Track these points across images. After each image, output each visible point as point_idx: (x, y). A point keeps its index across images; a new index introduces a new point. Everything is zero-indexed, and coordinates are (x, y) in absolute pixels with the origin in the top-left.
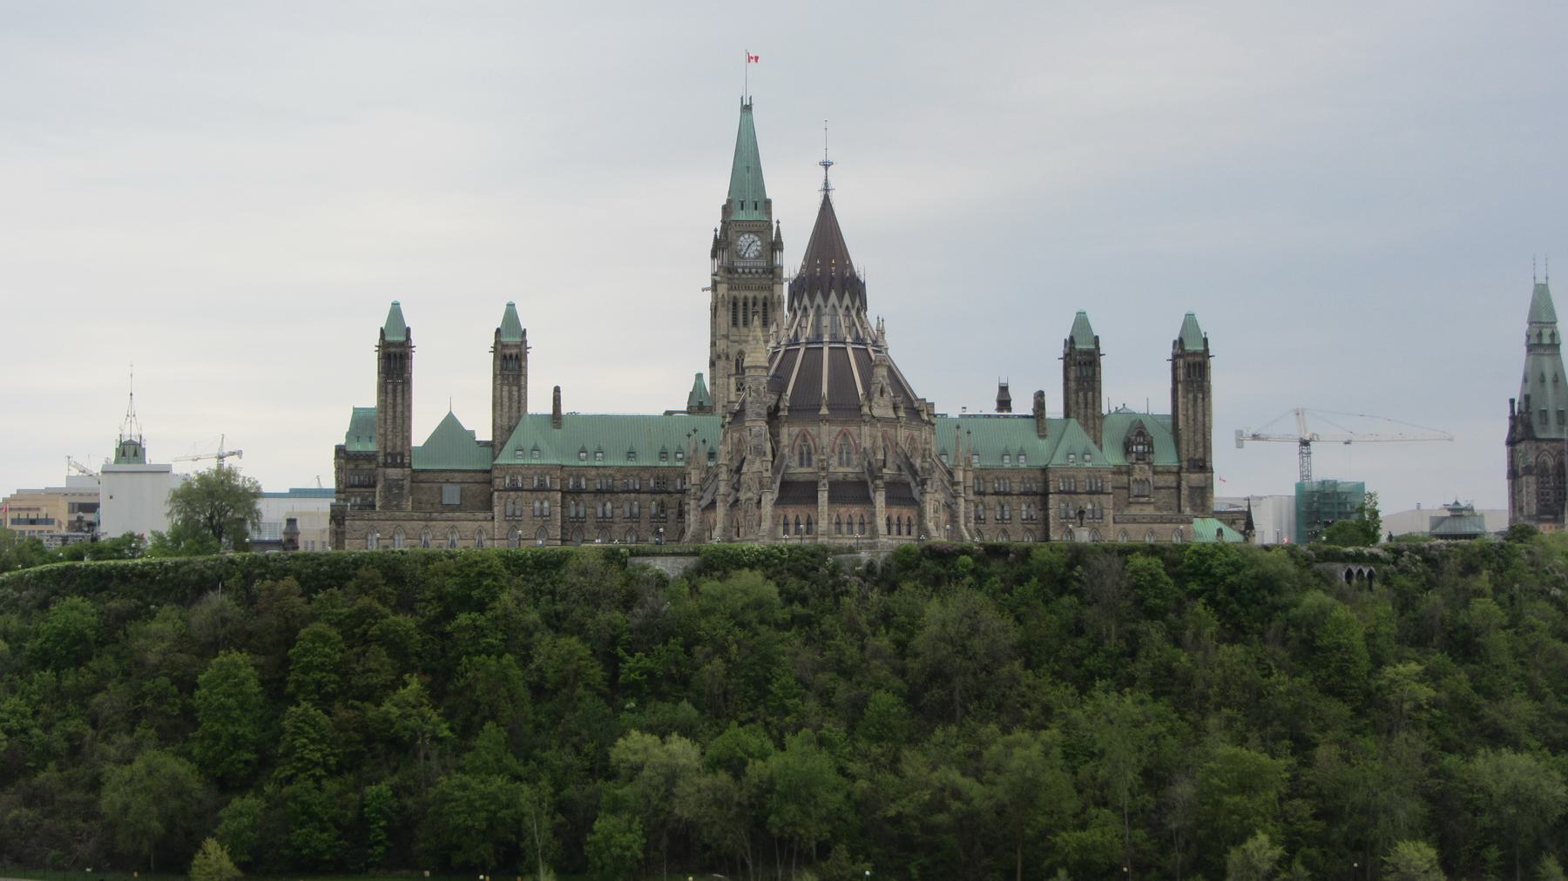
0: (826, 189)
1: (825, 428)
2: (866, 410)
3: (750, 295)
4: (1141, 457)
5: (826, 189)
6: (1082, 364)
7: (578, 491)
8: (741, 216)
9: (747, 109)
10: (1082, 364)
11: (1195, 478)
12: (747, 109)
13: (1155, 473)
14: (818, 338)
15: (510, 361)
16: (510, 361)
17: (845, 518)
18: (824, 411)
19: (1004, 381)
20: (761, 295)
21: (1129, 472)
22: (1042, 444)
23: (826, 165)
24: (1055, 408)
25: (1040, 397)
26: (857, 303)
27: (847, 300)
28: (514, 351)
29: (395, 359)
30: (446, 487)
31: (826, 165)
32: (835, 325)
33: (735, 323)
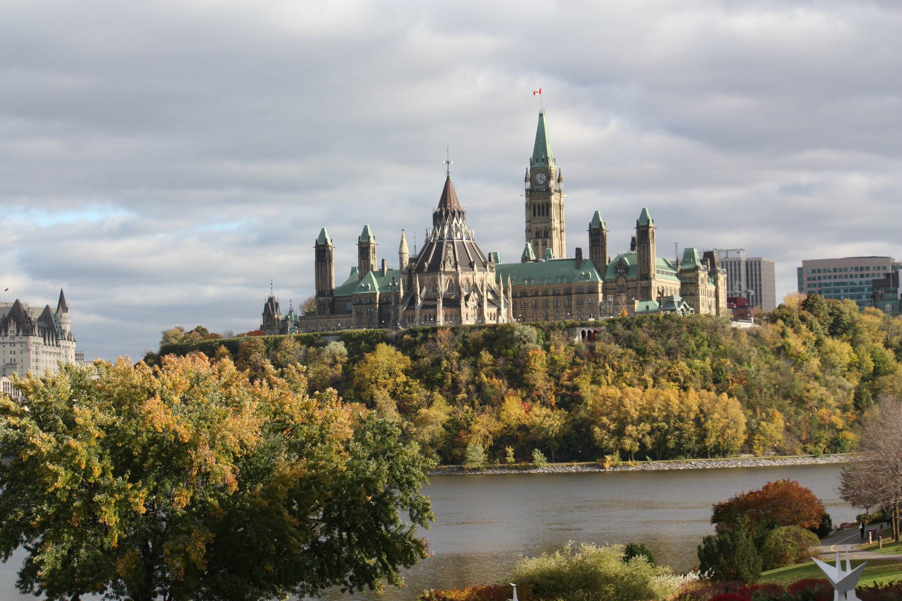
1: (426, 277)
2: (442, 269)
3: (540, 201)
4: (621, 274)
6: (597, 234)
8: (537, 165)
9: (541, 115)
10: (597, 234)
11: (644, 283)
13: (627, 281)
17: (428, 315)
18: (426, 270)
20: (545, 201)
21: (616, 281)
22: (576, 271)
23: (448, 163)
24: (586, 255)
25: (579, 251)
27: (461, 221)
31: (448, 163)
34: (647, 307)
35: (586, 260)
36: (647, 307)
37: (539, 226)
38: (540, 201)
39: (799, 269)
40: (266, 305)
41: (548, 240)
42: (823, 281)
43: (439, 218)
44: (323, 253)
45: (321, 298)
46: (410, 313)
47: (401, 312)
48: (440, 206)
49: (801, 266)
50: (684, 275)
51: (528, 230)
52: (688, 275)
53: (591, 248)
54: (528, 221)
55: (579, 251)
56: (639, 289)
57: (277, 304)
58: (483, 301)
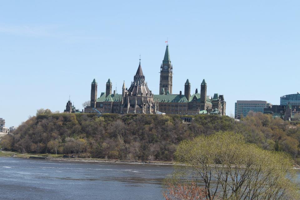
0: (140, 63)
5: (140, 63)
6: (187, 87)
7: (115, 105)
9: (167, 47)
10: (187, 87)
11: (202, 104)
12: (167, 47)
14: (137, 84)
15: (109, 86)
16: (109, 86)
19: (197, 88)
23: (140, 60)
24: (183, 93)
25: (181, 92)
26: (143, 80)
28: (108, 85)
29: (94, 87)
30: (101, 104)
31: (140, 60)
32: (140, 82)
33: (163, 79)
34: (203, 112)
35: (183, 95)
36: (203, 112)
37: (164, 83)
38: (165, 75)
39: (235, 103)
40: (67, 103)
41: (167, 88)
42: (244, 108)
43: (135, 78)
44: (94, 87)
45: (93, 102)
46: (125, 109)
47: (122, 108)
48: (137, 74)
49: (236, 102)
50: (214, 102)
51: (161, 84)
52: (215, 102)
53: (185, 91)
54: (161, 81)
55: (181, 92)
56: (200, 106)
57: (71, 103)
58: (150, 107)
